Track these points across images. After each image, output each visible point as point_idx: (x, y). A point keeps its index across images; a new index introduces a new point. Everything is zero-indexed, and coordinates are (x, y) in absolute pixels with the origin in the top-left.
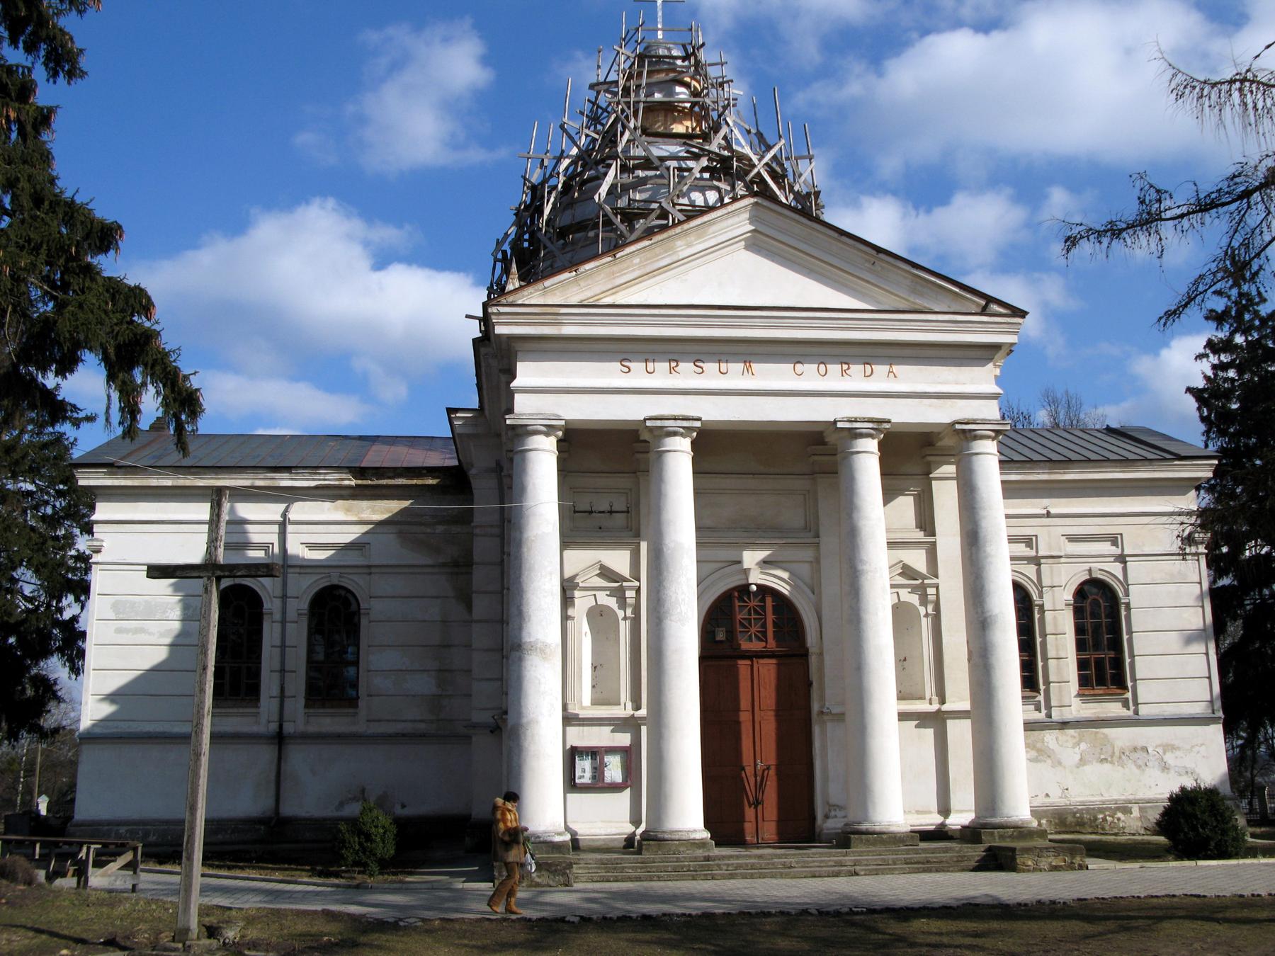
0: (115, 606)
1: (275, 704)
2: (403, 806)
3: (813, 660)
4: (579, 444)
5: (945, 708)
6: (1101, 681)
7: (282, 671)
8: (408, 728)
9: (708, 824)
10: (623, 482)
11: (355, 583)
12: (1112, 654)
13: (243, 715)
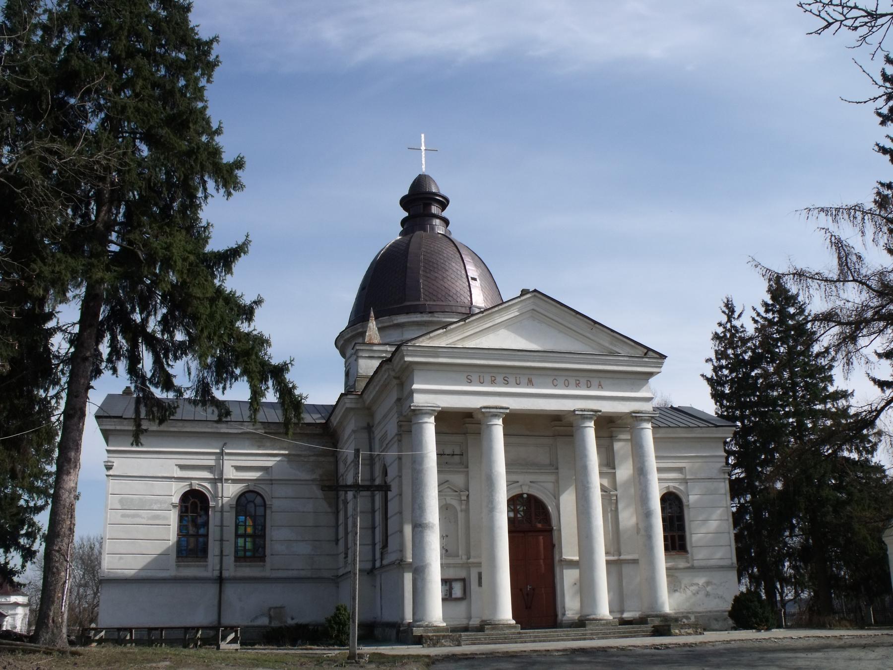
0: (121, 501)
1: (217, 560)
2: (292, 619)
3: (555, 534)
4: (444, 418)
5: (622, 557)
6: (674, 548)
7: (222, 540)
8: (295, 574)
9: (514, 618)
10: (458, 438)
11: (264, 489)
12: (676, 534)
13: (198, 566)
